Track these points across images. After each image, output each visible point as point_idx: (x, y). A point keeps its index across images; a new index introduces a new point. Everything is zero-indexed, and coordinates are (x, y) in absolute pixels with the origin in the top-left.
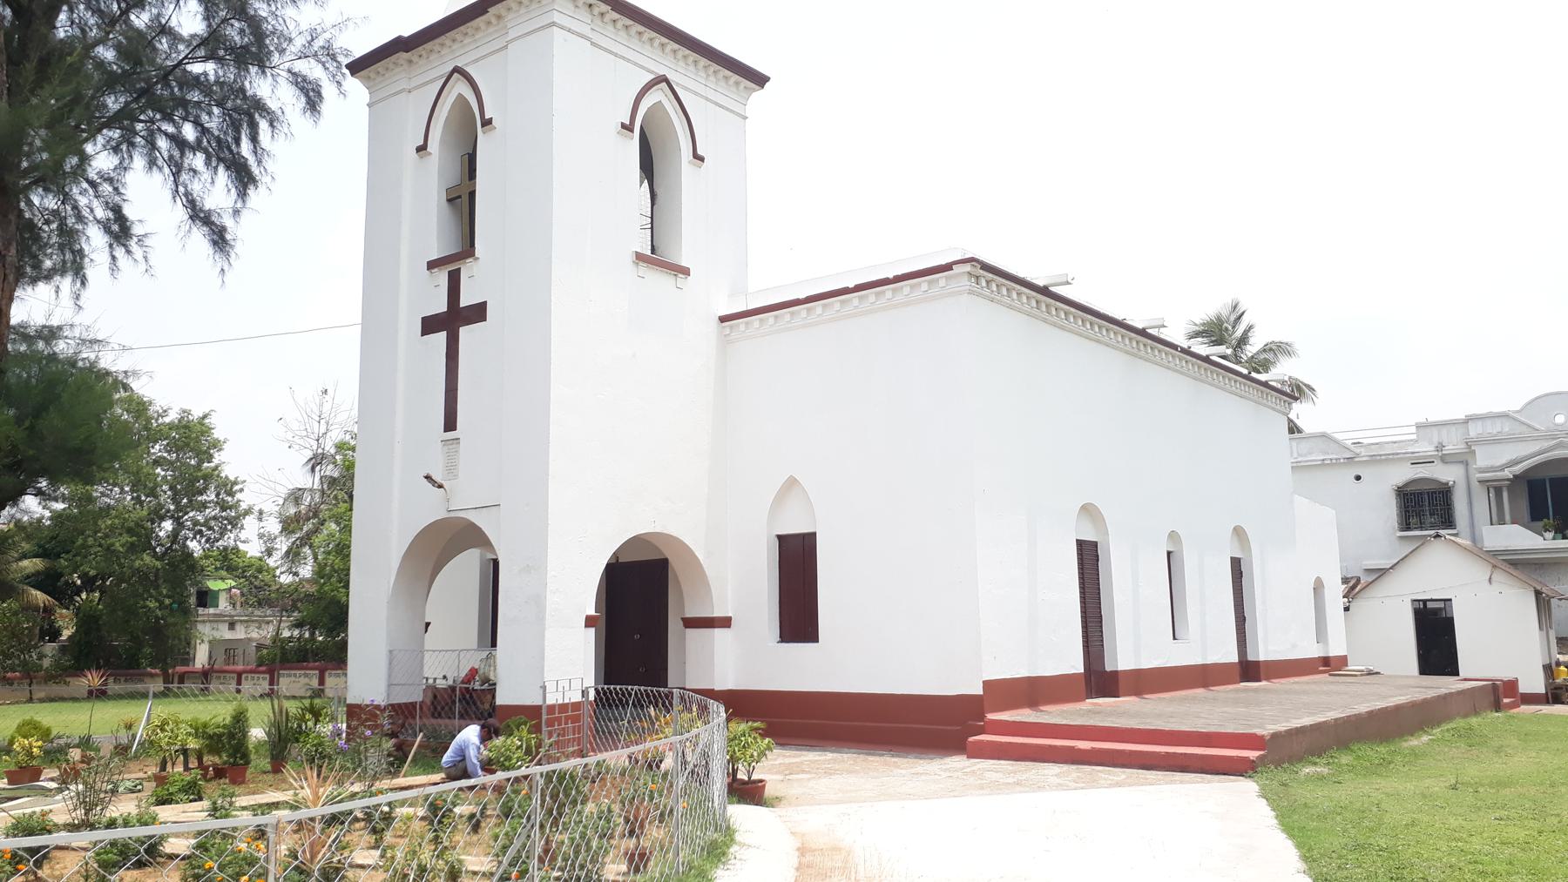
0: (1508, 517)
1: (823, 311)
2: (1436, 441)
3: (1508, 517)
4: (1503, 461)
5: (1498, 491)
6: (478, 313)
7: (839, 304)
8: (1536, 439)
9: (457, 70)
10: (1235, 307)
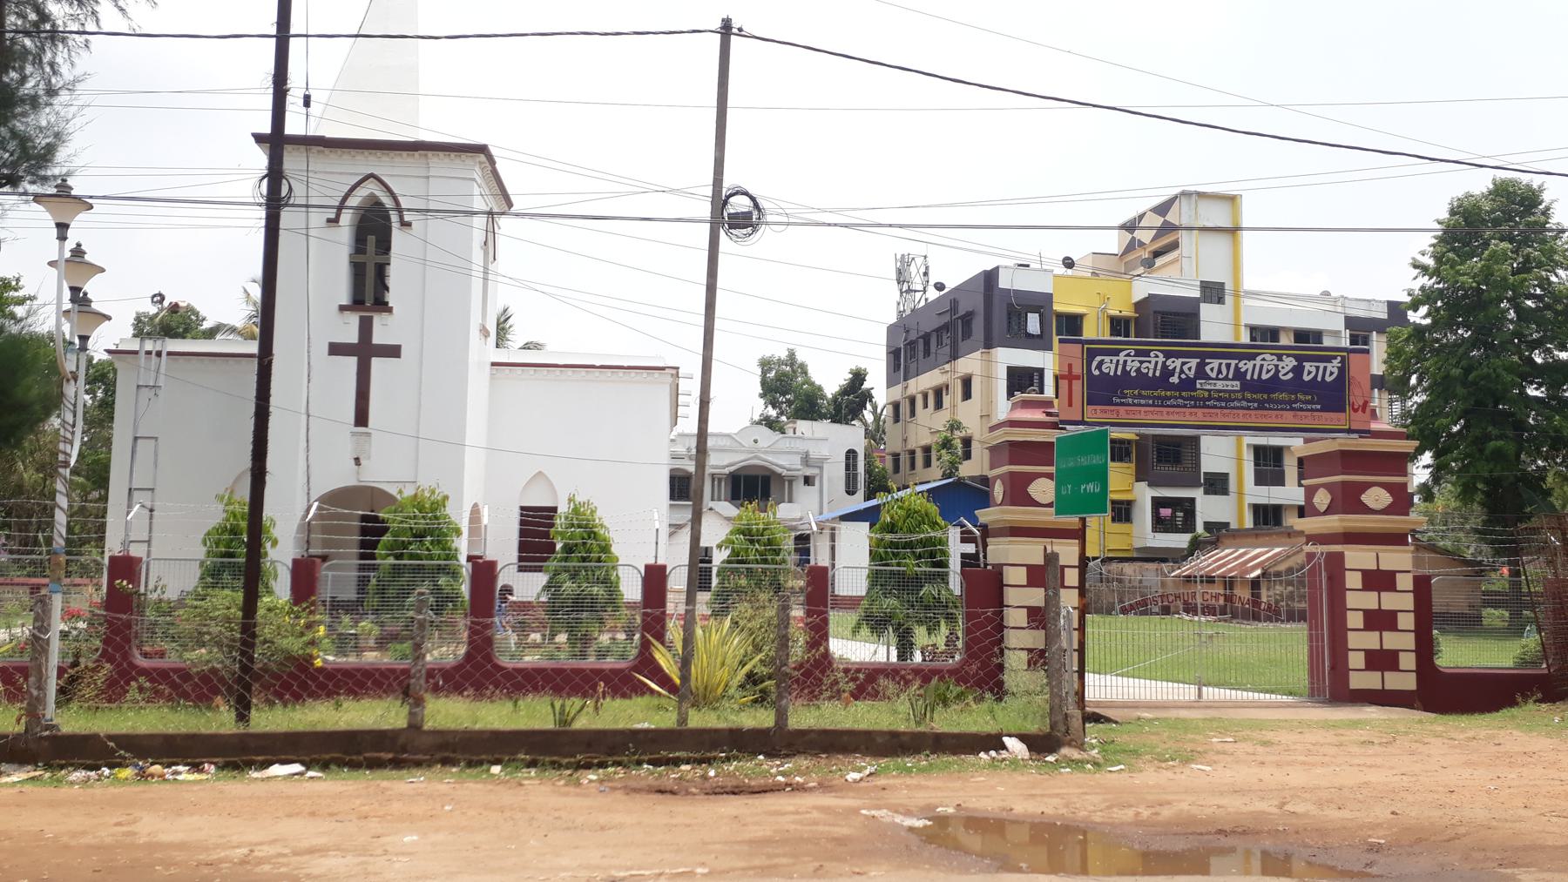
0: (723, 498)
3: (723, 498)
4: (725, 463)
5: (720, 480)
6: (393, 351)
8: (742, 452)
9: (372, 176)
10: (505, 311)
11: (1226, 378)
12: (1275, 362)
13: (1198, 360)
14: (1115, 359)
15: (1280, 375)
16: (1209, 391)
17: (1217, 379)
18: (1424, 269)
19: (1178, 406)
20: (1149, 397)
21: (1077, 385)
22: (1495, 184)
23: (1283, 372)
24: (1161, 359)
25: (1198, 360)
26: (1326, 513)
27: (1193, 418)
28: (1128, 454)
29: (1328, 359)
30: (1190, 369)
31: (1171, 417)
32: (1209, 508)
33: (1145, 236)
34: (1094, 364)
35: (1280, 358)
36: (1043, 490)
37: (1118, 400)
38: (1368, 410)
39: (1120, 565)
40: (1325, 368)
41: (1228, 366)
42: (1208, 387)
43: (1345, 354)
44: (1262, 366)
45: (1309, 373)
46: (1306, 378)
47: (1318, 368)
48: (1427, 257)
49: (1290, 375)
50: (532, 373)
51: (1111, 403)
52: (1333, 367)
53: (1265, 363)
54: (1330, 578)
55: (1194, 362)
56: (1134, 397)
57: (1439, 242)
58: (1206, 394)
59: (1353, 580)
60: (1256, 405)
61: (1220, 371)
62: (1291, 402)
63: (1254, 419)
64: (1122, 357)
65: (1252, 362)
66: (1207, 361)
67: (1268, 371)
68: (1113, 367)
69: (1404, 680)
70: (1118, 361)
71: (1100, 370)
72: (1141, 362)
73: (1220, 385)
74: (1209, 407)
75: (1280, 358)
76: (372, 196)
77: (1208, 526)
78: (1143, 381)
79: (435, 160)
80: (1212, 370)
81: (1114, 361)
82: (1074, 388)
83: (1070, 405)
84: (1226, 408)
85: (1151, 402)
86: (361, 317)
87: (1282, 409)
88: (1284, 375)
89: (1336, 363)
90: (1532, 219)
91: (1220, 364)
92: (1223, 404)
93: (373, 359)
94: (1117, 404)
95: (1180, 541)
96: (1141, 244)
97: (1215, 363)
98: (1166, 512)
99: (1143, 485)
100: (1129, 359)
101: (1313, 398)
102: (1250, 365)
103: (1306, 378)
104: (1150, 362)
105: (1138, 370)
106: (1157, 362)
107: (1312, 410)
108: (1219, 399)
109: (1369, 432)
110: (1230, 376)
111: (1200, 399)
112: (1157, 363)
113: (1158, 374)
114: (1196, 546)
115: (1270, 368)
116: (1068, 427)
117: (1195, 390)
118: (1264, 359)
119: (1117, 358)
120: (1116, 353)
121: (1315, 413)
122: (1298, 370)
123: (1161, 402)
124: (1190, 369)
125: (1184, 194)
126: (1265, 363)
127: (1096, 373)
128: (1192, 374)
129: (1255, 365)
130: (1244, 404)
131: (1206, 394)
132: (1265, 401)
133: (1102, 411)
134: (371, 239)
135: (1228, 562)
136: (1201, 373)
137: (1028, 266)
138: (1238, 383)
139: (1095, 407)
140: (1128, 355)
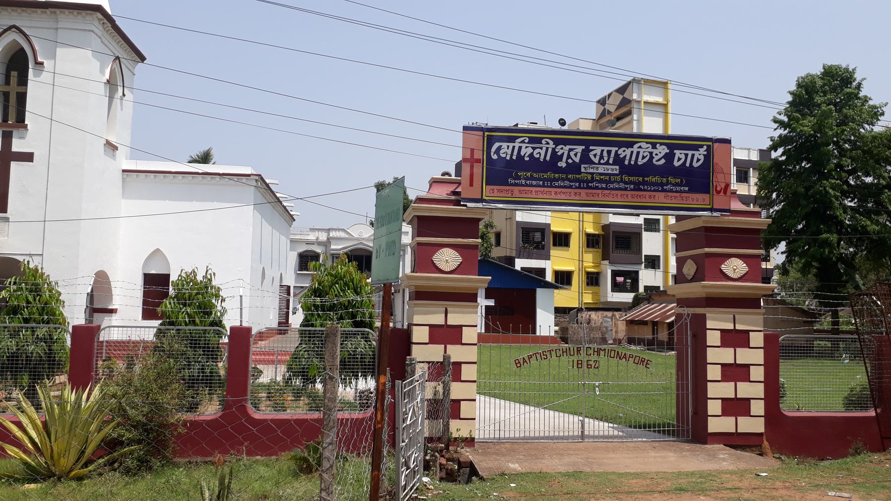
1: (182, 179)
2: (317, 235)
6: (28, 157)
7: (191, 178)
9: (14, 27)
11: (607, 163)
12: (650, 150)
13: (584, 147)
14: (511, 145)
15: (654, 161)
16: (592, 174)
17: (599, 163)
18: (781, 124)
19: (565, 187)
20: (540, 179)
21: (478, 169)
22: (824, 68)
23: (656, 158)
24: (551, 145)
25: (584, 147)
26: (692, 280)
27: (577, 198)
28: (598, 243)
29: (696, 148)
30: (576, 155)
31: (558, 196)
32: (648, 278)
33: (612, 109)
34: (494, 149)
35: (654, 146)
36: (447, 259)
37: (513, 181)
38: (728, 193)
39: (589, 313)
40: (693, 155)
41: (609, 152)
42: (591, 171)
43: (711, 143)
44: (638, 153)
45: (679, 159)
46: (676, 164)
47: (686, 155)
48: (782, 115)
49: (663, 161)
50: (162, 178)
51: (507, 184)
52: (700, 154)
53: (641, 151)
54: (694, 336)
55: (580, 149)
56: (527, 179)
57: (790, 106)
58: (589, 177)
59: (713, 338)
60: (632, 186)
61: (602, 157)
62: (662, 184)
63: (630, 199)
64: (517, 145)
65: (630, 150)
66: (591, 148)
67: (644, 158)
68: (509, 152)
69: (753, 424)
70: (514, 147)
71: (498, 155)
72: (534, 149)
73: (601, 169)
74: (591, 188)
75: (654, 146)
76: (15, 42)
77: (646, 288)
78: (534, 164)
79: (62, 16)
80: (595, 156)
81: (511, 148)
82: (475, 170)
83: (471, 184)
84: (606, 189)
85: (541, 183)
86: (3, 131)
87: (654, 191)
88: (656, 161)
89: (703, 151)
90: (848, 90)
91: (602, 151)
92: (604, 186)
93: (12, 162)
94: (512, 185)
95: (627, 297)
96: (609, 112)
97: (598, 150)
98: (620, 279)
99: (606, 262)
100: (524, 145)
101: (682, 181)
102: (628, 152)
103: (676, 164)
104: (541, 148)
105: (531, 156)
106: (547, 149)
107: (681, 192)
108: (601, 181)
109: (729, 211)
110: (611, 161)
111: (584, 181)
112: (547, 149)
113: (548, 158)
114: (637, 301)
115: (645, 155)
116: (469, 205)
117: (580, 173)
118: (640, 147)
119: (514, 144)
120: (512, 140)
121: (684, 195)
122: (669, 157)
123: (550, 183)
124: (576, 155)
125: (634, 80)
126: (641, 151)
127: (495, 157)
128: (577, 160)
129: (632, 152)
130: (622, 185)
131: (589, 177)
132: (640, 183)
133: (498, 190)
134: (14, 74)
135: (656, 312)
136: (585, 158)
137: (536, 124)
138: (617, 167)
139: (492, 187)
140: (523, 142)
